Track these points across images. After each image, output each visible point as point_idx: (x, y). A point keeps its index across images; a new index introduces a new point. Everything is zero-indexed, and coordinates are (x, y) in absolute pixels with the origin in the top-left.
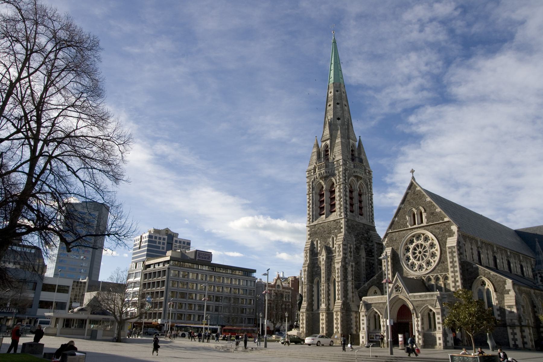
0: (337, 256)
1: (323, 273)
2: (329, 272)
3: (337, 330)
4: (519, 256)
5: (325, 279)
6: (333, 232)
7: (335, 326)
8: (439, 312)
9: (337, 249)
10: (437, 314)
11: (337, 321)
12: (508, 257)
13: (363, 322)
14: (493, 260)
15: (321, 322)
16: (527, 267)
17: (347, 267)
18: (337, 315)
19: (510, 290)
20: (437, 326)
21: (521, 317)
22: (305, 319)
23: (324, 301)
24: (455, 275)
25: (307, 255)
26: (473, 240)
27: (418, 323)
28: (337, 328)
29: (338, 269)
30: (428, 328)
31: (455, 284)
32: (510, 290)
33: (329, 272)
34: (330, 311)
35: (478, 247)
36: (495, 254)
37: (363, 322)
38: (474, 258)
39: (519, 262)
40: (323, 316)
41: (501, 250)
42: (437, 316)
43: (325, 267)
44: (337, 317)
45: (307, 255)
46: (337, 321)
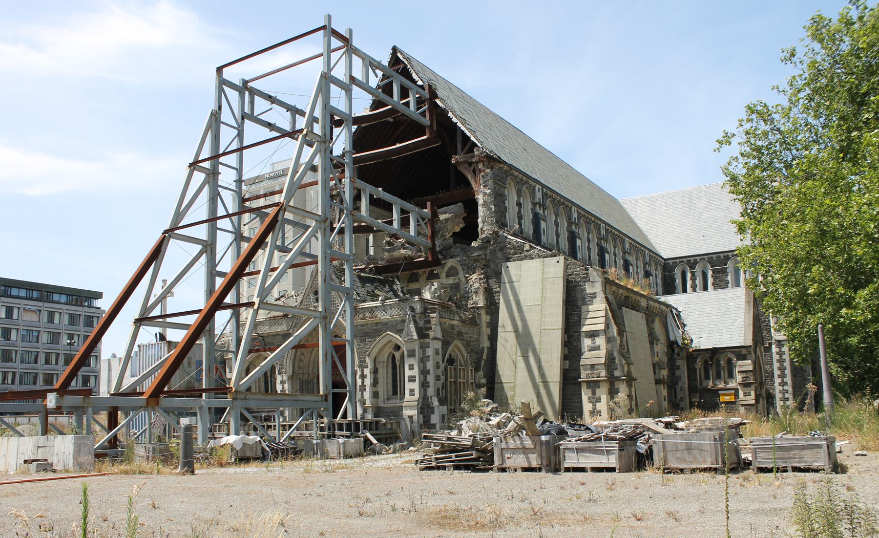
4: (623, 242)
8: (414, 351)
10: (409, 356)
12: (601, 239)
14: (568, 241)
16: (637, 267)
19: (594, 296)
20: (409, 386)
21: (614, 359)
26: (524, 184)
27: (363, 383)
30: (391, 393)
32: (595, 293)
35: (534, 204)
36: (574, 227)
38: (523, 227)
39: (621, 254)
41: (588, 223)
42: (408, 362)
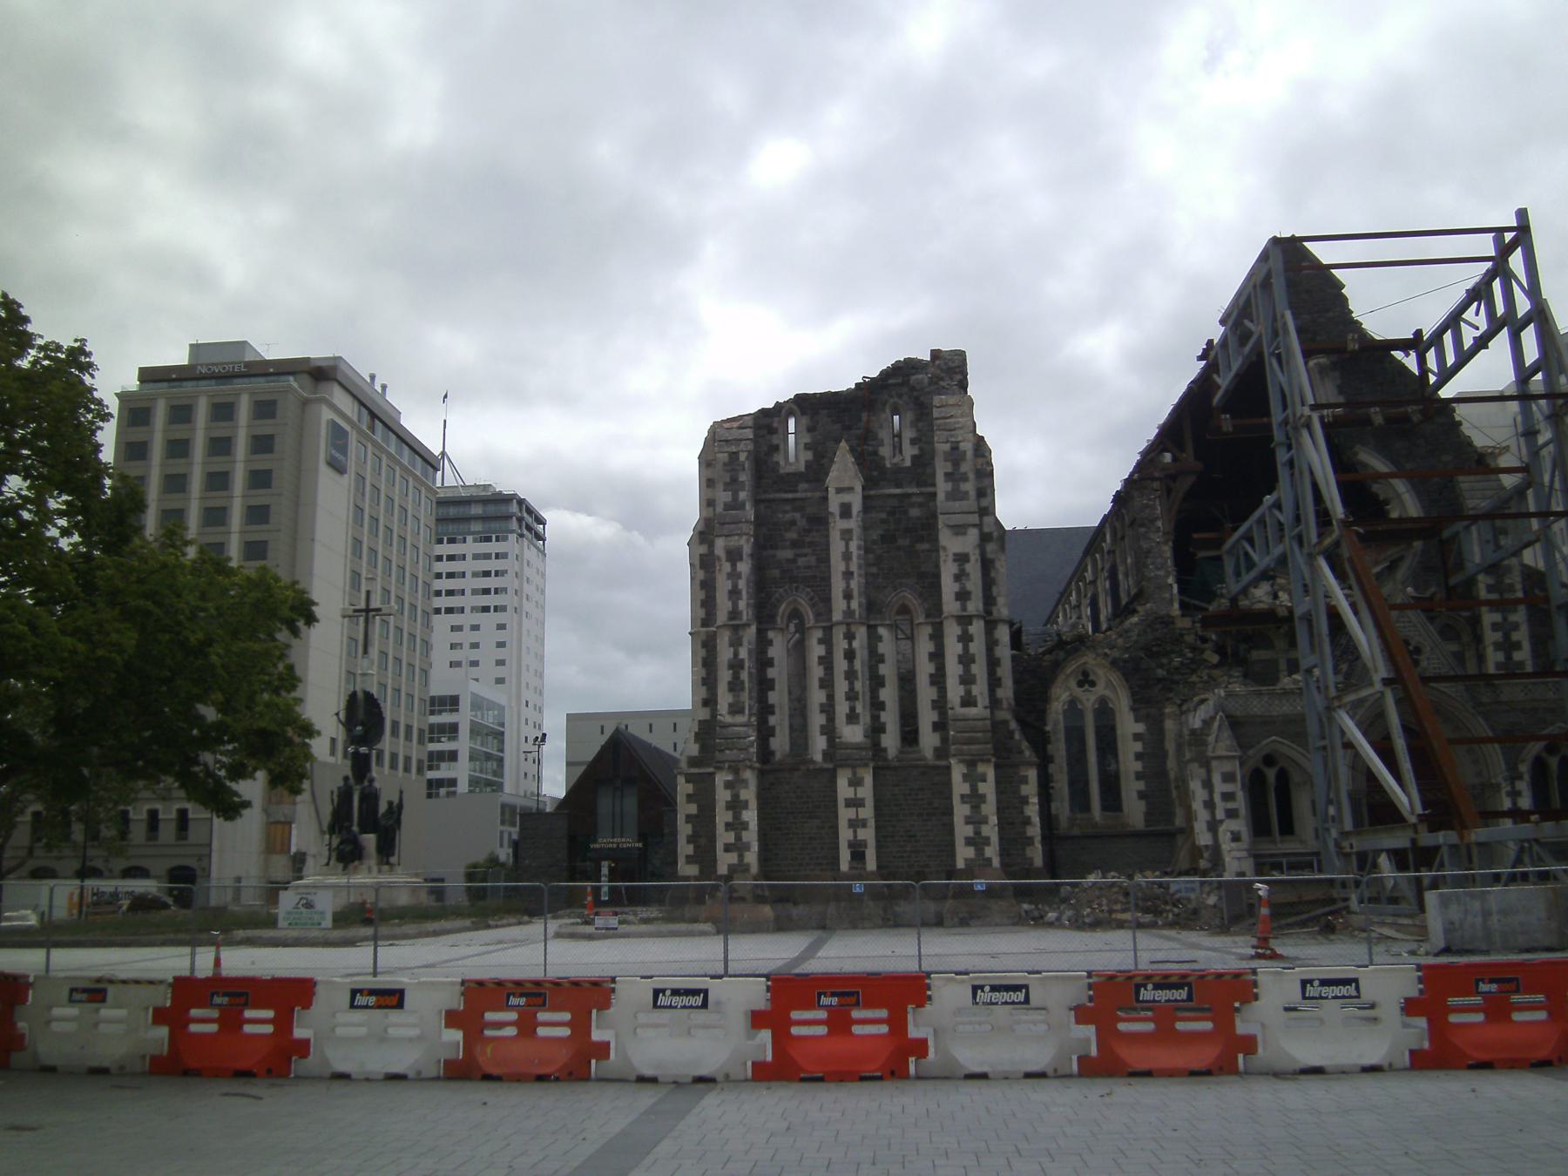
0: (941, 496)
1: (848, 575)
2: (874, 570)
3: (980, 853)
5: (860, 606)
6: (902, 384)
7: (962, 830)
9: (941, 468)
11: (976, 808)
13: (1230, 805)
15: (845, 814)
17: (990, 556)
18: (972, 778)
22: (753, 804)
23: (859, 709)
24: (1505, 619)
25: (734, 480)
28: (977, 841)
29: (961, 558)
31: (1509, 657)
33: (874, 570)
34: (886, 759)
37: (1230, 805)
40: (855, 782)
43: (859, 548)
44: (974, 789)
45: (734, 480)
46: (976, 808)
